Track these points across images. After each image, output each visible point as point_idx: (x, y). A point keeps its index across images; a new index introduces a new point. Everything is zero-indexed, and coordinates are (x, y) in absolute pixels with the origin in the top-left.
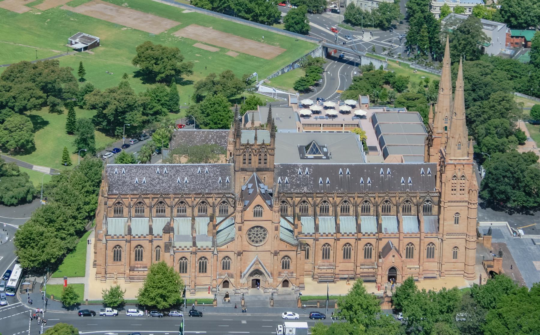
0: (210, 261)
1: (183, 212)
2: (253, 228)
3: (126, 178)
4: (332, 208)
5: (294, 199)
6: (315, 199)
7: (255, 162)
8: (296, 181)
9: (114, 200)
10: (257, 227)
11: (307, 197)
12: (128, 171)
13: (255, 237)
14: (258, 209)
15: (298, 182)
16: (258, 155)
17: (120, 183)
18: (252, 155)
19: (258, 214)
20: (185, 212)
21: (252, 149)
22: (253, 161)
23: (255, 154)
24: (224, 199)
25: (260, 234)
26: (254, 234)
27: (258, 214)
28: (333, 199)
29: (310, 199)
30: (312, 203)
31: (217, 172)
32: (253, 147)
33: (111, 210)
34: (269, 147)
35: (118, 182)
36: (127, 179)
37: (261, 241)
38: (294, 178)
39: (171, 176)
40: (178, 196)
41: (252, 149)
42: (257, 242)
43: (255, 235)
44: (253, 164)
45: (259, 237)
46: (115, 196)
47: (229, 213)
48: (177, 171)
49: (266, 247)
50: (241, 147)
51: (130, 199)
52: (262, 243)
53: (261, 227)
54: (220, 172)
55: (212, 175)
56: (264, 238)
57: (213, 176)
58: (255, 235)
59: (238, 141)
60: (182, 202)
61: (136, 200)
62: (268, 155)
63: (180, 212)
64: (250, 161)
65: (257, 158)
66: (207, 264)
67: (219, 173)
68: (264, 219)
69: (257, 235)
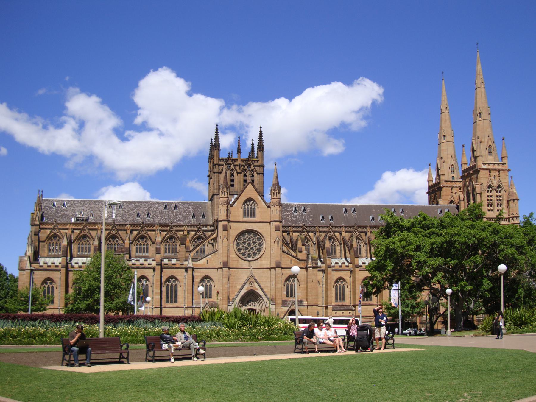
0: (182, 284)
1: (144, 252)
2: (243, 233)
3: (67, 211)
4: (339, 248)
5: (291, 234)
6: (317, 234)
7: (239, 182)
8: (291, 217)
9: (49, 231)
10: (249, 231)
11: (308, 232)
12: (71, 205)
13: (246, 248)
14: (249, 205)
15: (294, 219)
16: (243, 174)
17: (58, 215)
18: (235, 174)
19: (249, 213)
20: (147, 252)
21: (235, 166)
22: (235, 183)
23: (239, 171)
24: (199, 234)
25: (254, 243)
26: (244, 243)
27: (249, 213)
28: (341, 234)
29: (311, 234)
30: (314, 239)
31: (189, 208)
32: (236, 163)
33: (44, 246)
34: (256, 164)
35: (55, 215)
36: (68, 212)
37: (255, 254)
38: (288, 215)
39: (128, 211)
40: (137, 228)
41: (235, 166)
42: (249, 255)
43: (246, 245)
44: (236, 186)
45: (252, 248)
46: (50, 227)
47: (206, 253)
48: (136, 206)
49: (263, 262)
50: (220, 163)
51: (70, 231)
52: (258, 256)
53: (255, 232)
54: (193, 208)
55: (182, 211)
56: (259, 250)
57: (184, 212)
58: (246, 245)
59: (216, 152)
60: (142, 237)
61: (78, 232)
62: (255, 174)
63: (140, 252)
64: (232, 183)
65: (242, 178)
66: (179, 289)
67: (192, 209)
68: (258, 220)
69: (249, 244)
